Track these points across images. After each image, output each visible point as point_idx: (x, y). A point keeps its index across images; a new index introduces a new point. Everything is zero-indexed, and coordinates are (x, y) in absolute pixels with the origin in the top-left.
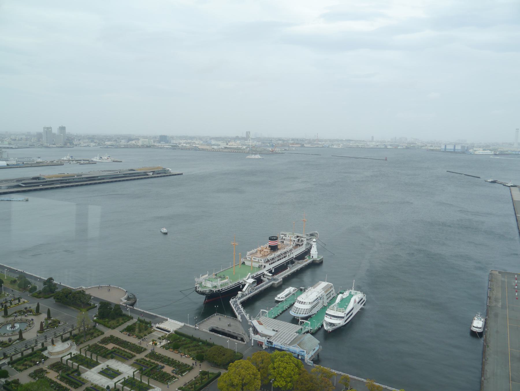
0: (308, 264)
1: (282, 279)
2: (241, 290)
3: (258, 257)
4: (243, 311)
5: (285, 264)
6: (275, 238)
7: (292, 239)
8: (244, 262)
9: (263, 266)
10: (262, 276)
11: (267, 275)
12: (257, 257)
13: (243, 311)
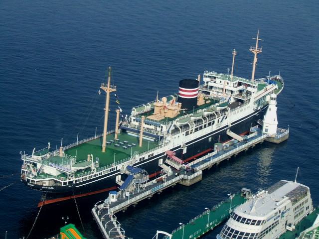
0: (256, 145)
4: (120, 232)
5: (210, 139)
10: (162, 160)
13: (120, 232)
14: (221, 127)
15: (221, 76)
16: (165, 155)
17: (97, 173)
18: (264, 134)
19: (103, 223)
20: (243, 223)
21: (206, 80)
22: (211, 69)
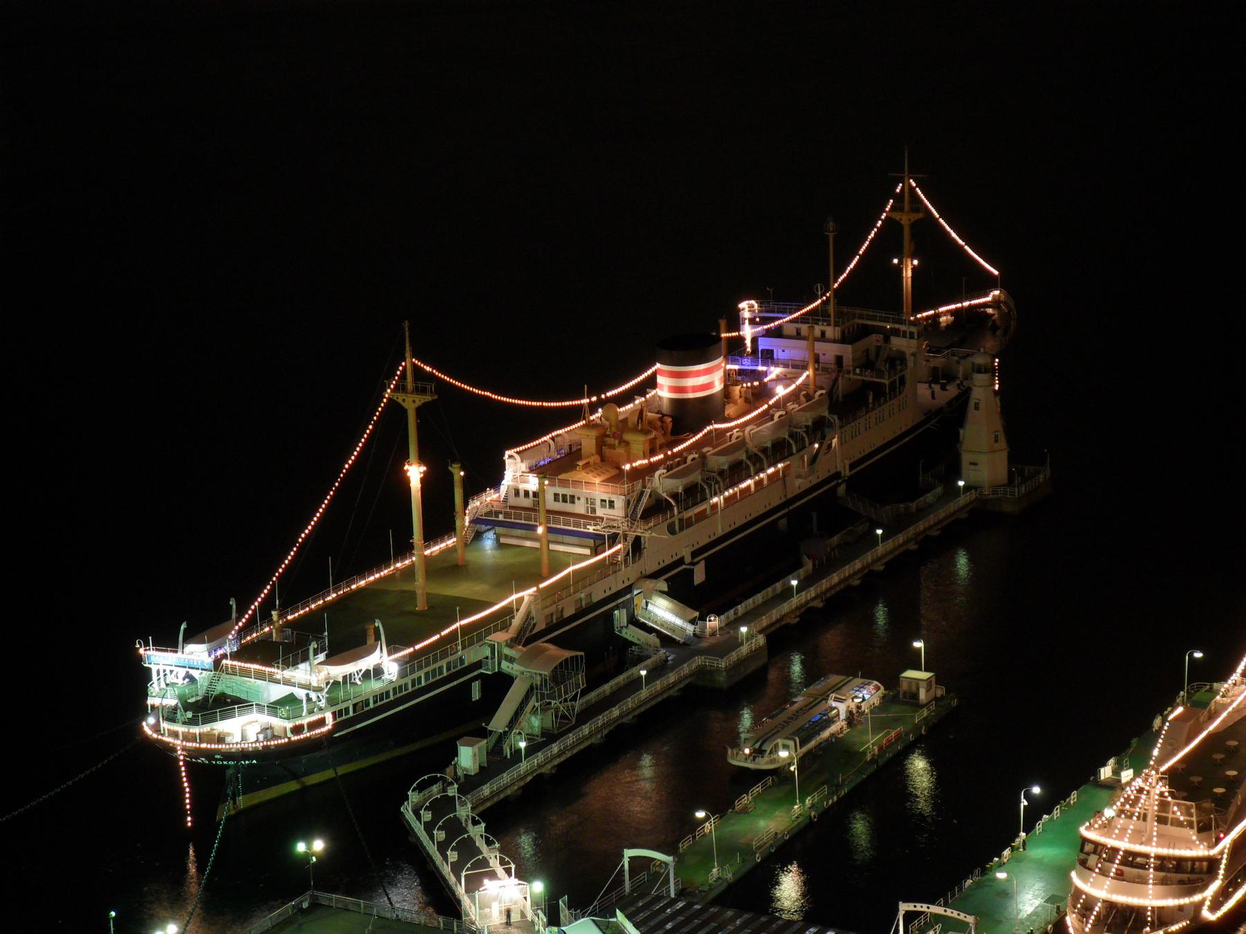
5: (784, 522)
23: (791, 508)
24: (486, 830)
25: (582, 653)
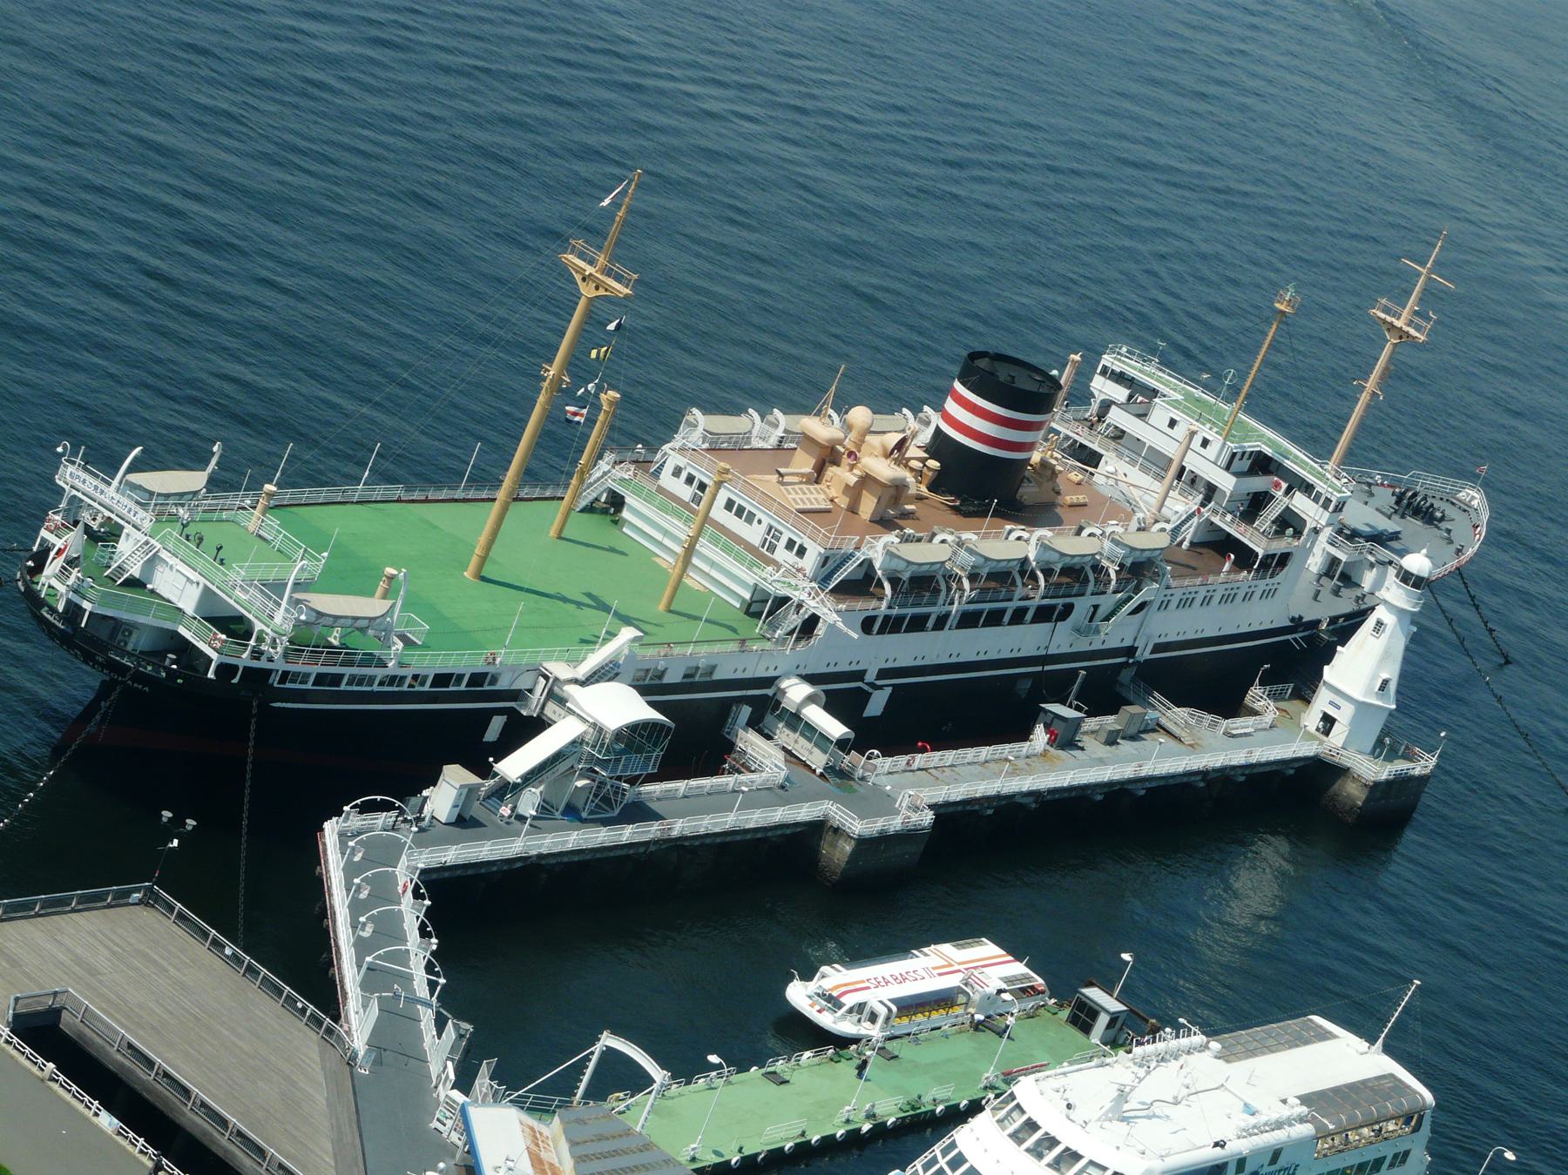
1: (928, 818)
2: (480, 760)
3: (783, 511)
4: (420, 978)
5: (1027, 685)
6: (1025, 383)
7: (1194, 463)
8: (617, 502)
9: (794, 620)
10: (746, 711)
11: (795, 721)
12: (766, 500)
14: (1097, 646)
15: (1188, 396)
16: (769, 692)
17: (401, 672)
18: (1308, 736)
19: (356, 908)
20: (1040, 1156)
21: (1102, 387)
22: (1147, 351)
23: (1047, 668)
24: (429, 913)
25: (673, 725)
